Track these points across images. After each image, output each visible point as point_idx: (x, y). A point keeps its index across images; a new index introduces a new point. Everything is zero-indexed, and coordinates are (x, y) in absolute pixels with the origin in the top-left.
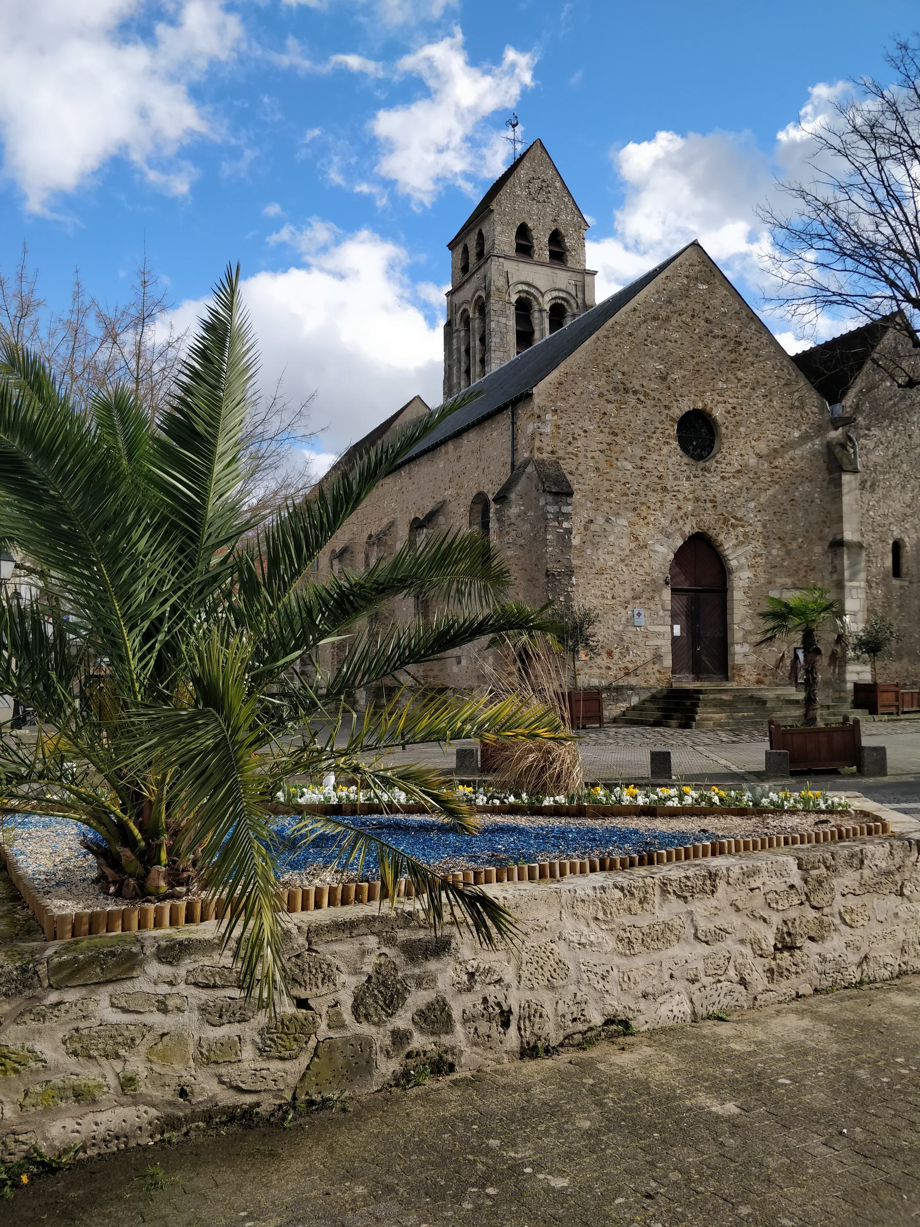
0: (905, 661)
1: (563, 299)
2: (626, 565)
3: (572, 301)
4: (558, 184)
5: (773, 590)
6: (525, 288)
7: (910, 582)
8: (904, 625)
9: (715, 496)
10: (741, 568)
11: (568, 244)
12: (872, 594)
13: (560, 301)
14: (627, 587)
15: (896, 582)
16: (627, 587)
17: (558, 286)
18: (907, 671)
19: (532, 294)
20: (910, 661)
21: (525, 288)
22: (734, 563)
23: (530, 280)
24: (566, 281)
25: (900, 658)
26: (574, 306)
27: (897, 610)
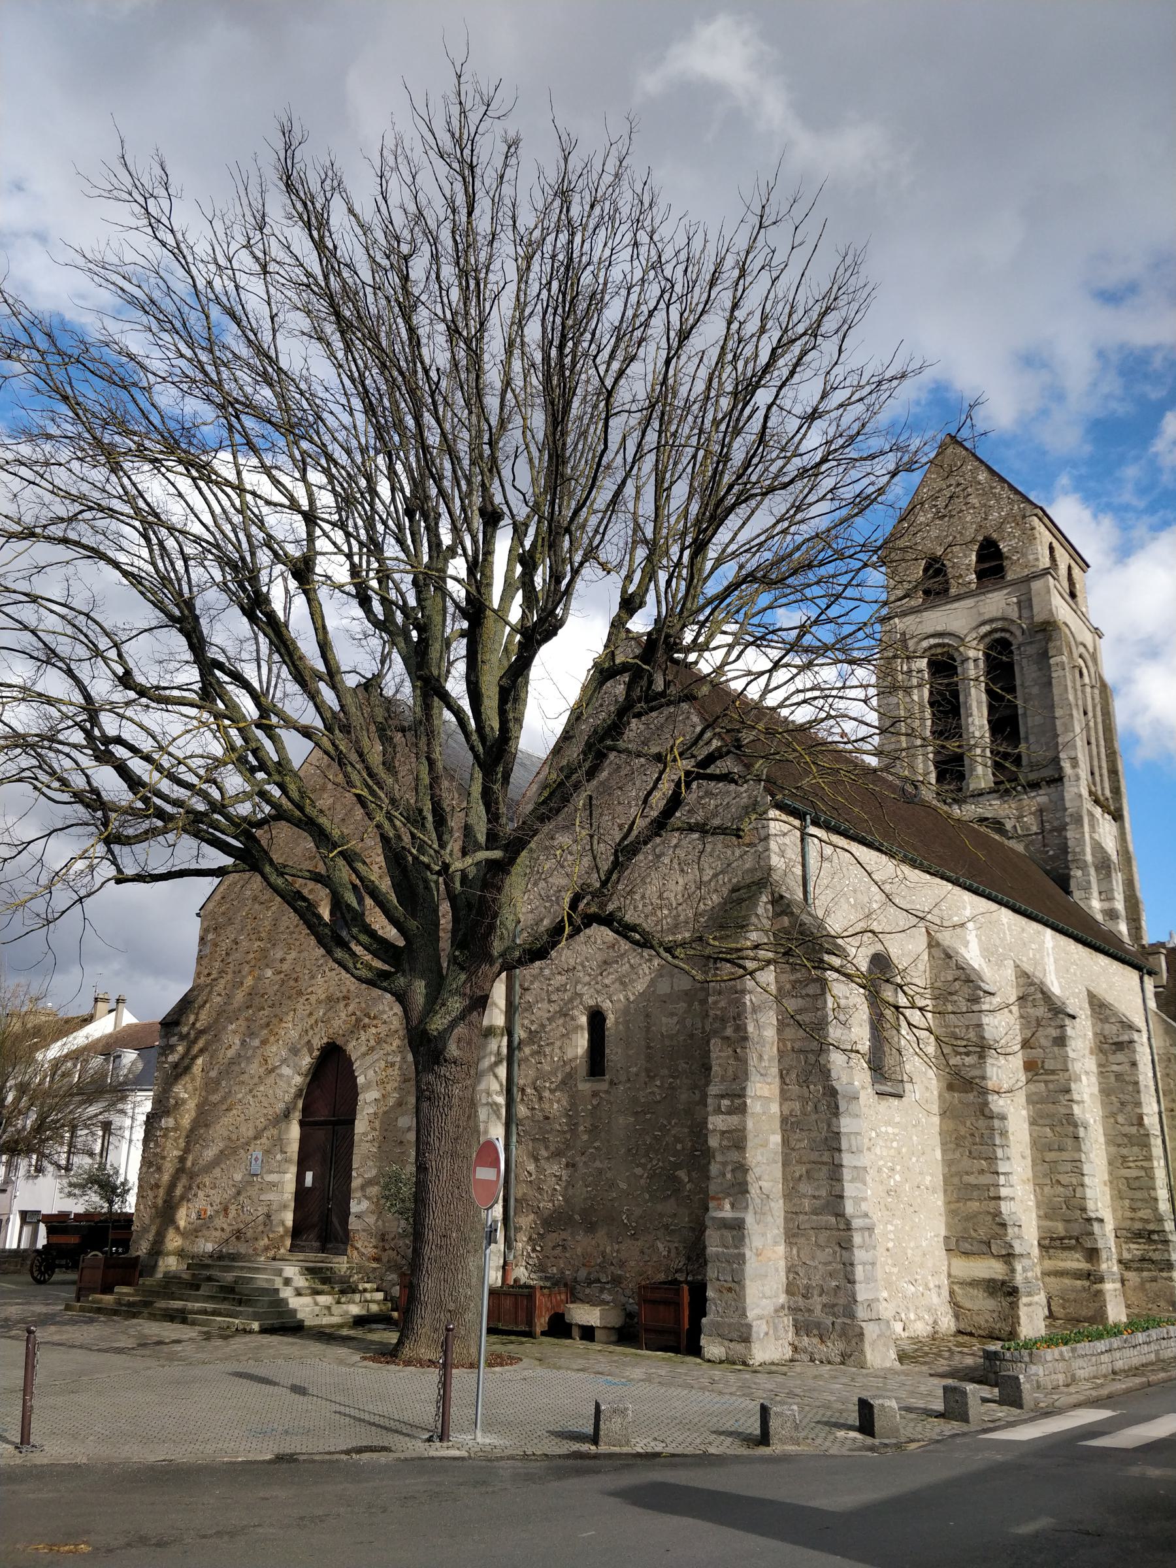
0: (601, 1233)
1: (1003, 630)
2: (254, 1097)
3: (1013, 628)
4: (982, 476)
5: (403, 1115)
6: (932, 641)
7: (612, 1083)
8: (598, 1164)
9: (348, 991)
10: (368, 1086)
11: (1005, 550)
12: (542, 1110)
13: (997, 635)
14: (251, 1125)
15: (585, 1087)
16: (251, 1125)
17: (987, 617)
18: (603, 1254)
19: (949, 645)
20: (609, 1235)
21: (932, 641)
22: (361, 1080)
23: (939, 628)
24: (1003, 604)
25: (591, 1228)
26: (1018, 633)
27: (585, 1137)
